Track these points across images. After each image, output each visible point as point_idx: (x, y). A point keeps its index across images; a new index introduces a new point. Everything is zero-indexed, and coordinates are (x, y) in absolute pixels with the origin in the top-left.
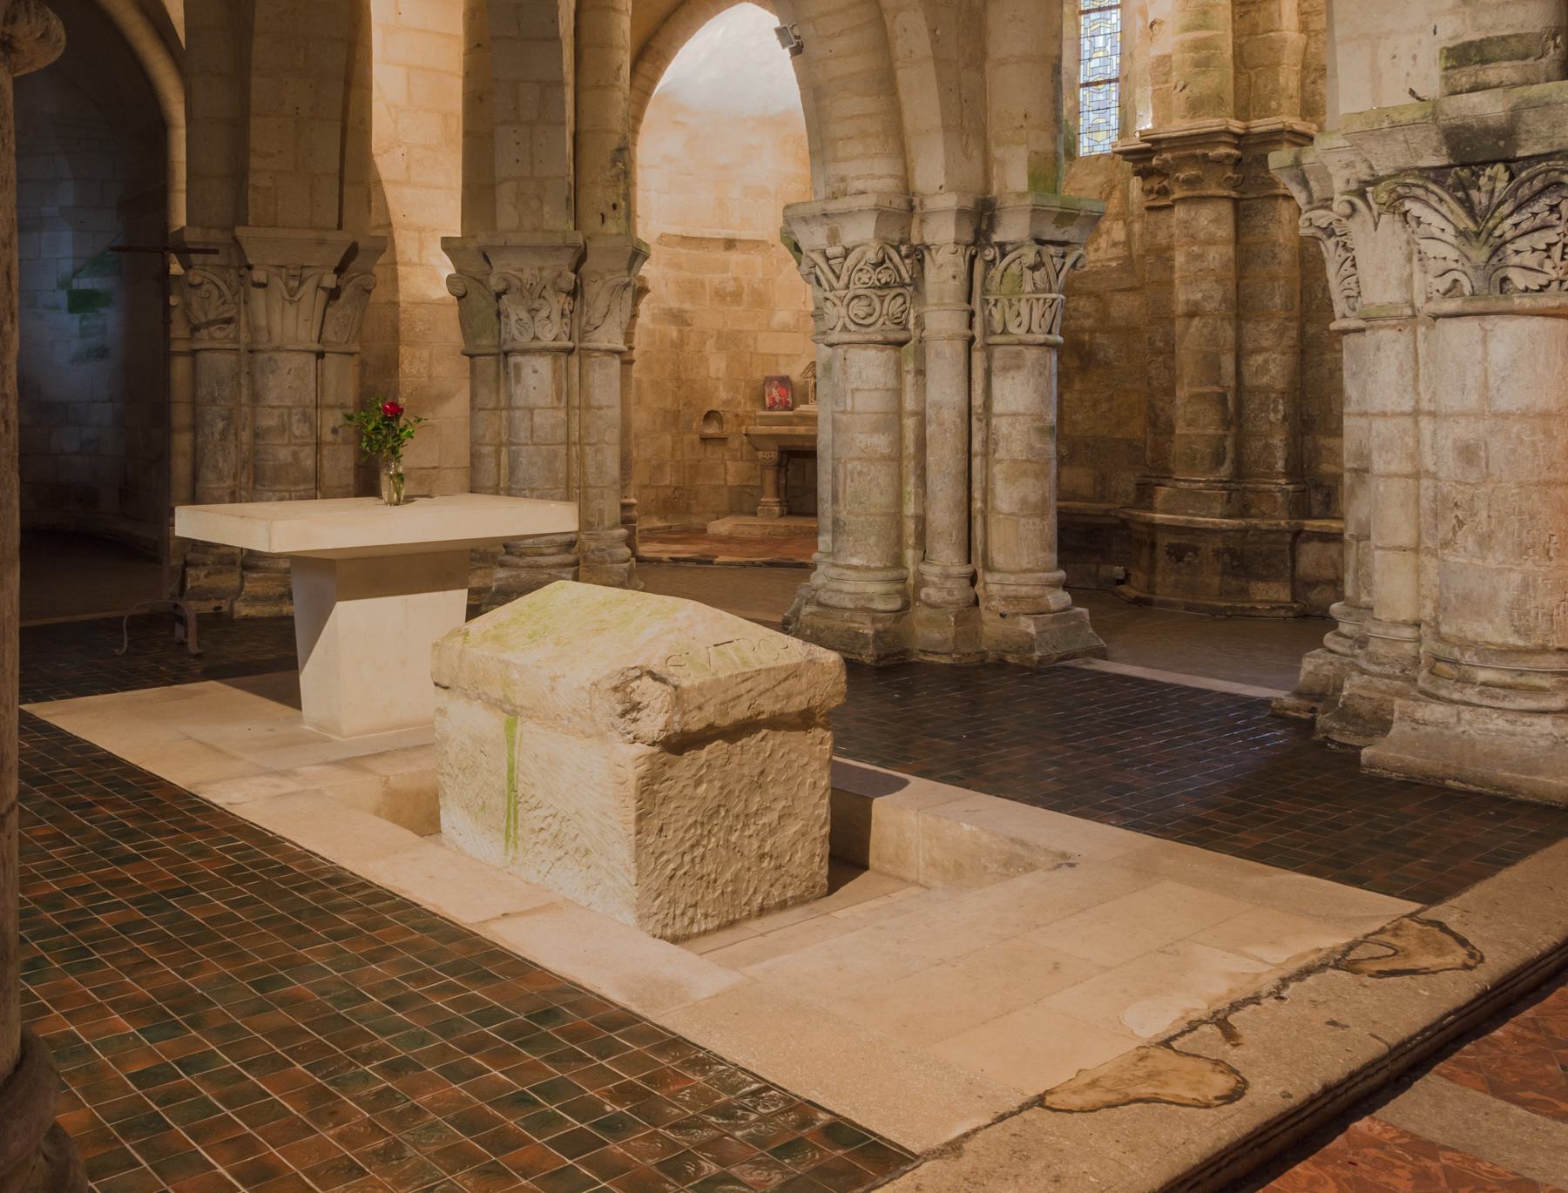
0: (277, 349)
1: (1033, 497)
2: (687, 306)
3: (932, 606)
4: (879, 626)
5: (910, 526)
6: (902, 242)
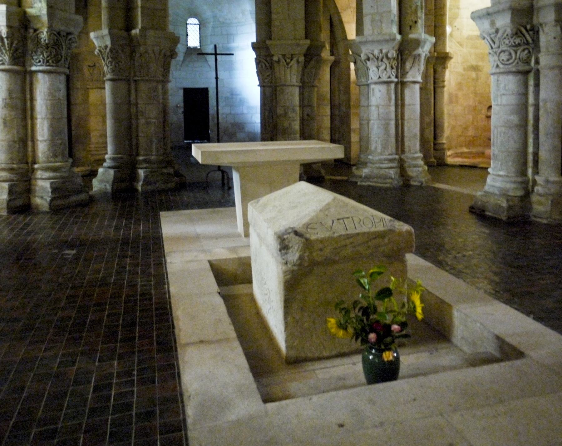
0: (285, 85)
2: (480, 64)
3: (540, 195)
5: (530, 158)
6: (527, 23)
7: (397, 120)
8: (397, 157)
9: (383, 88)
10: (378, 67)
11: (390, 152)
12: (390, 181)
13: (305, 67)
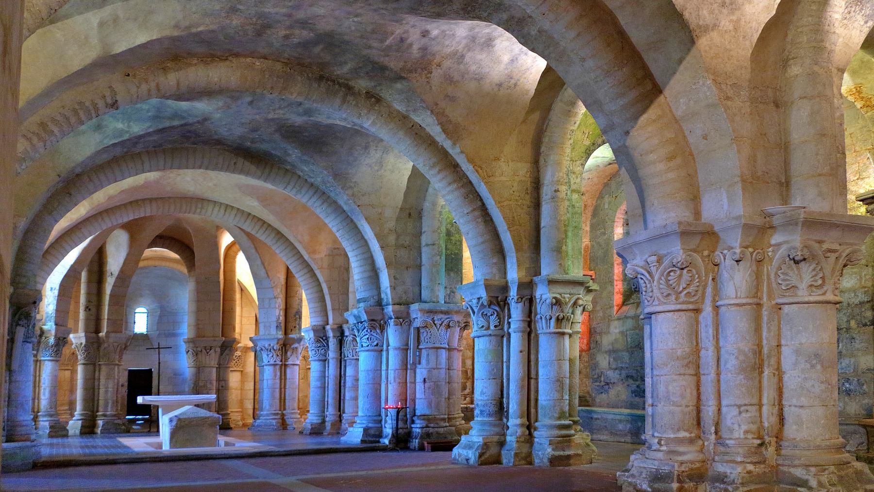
1: (353, 396)
4: (313, 426)
7: (281, 389)
8: (280, 412)
9: (271, 368)
10: (268, 355)
11: (274, 409)
12: (272, 427)
13: (221, 354)
